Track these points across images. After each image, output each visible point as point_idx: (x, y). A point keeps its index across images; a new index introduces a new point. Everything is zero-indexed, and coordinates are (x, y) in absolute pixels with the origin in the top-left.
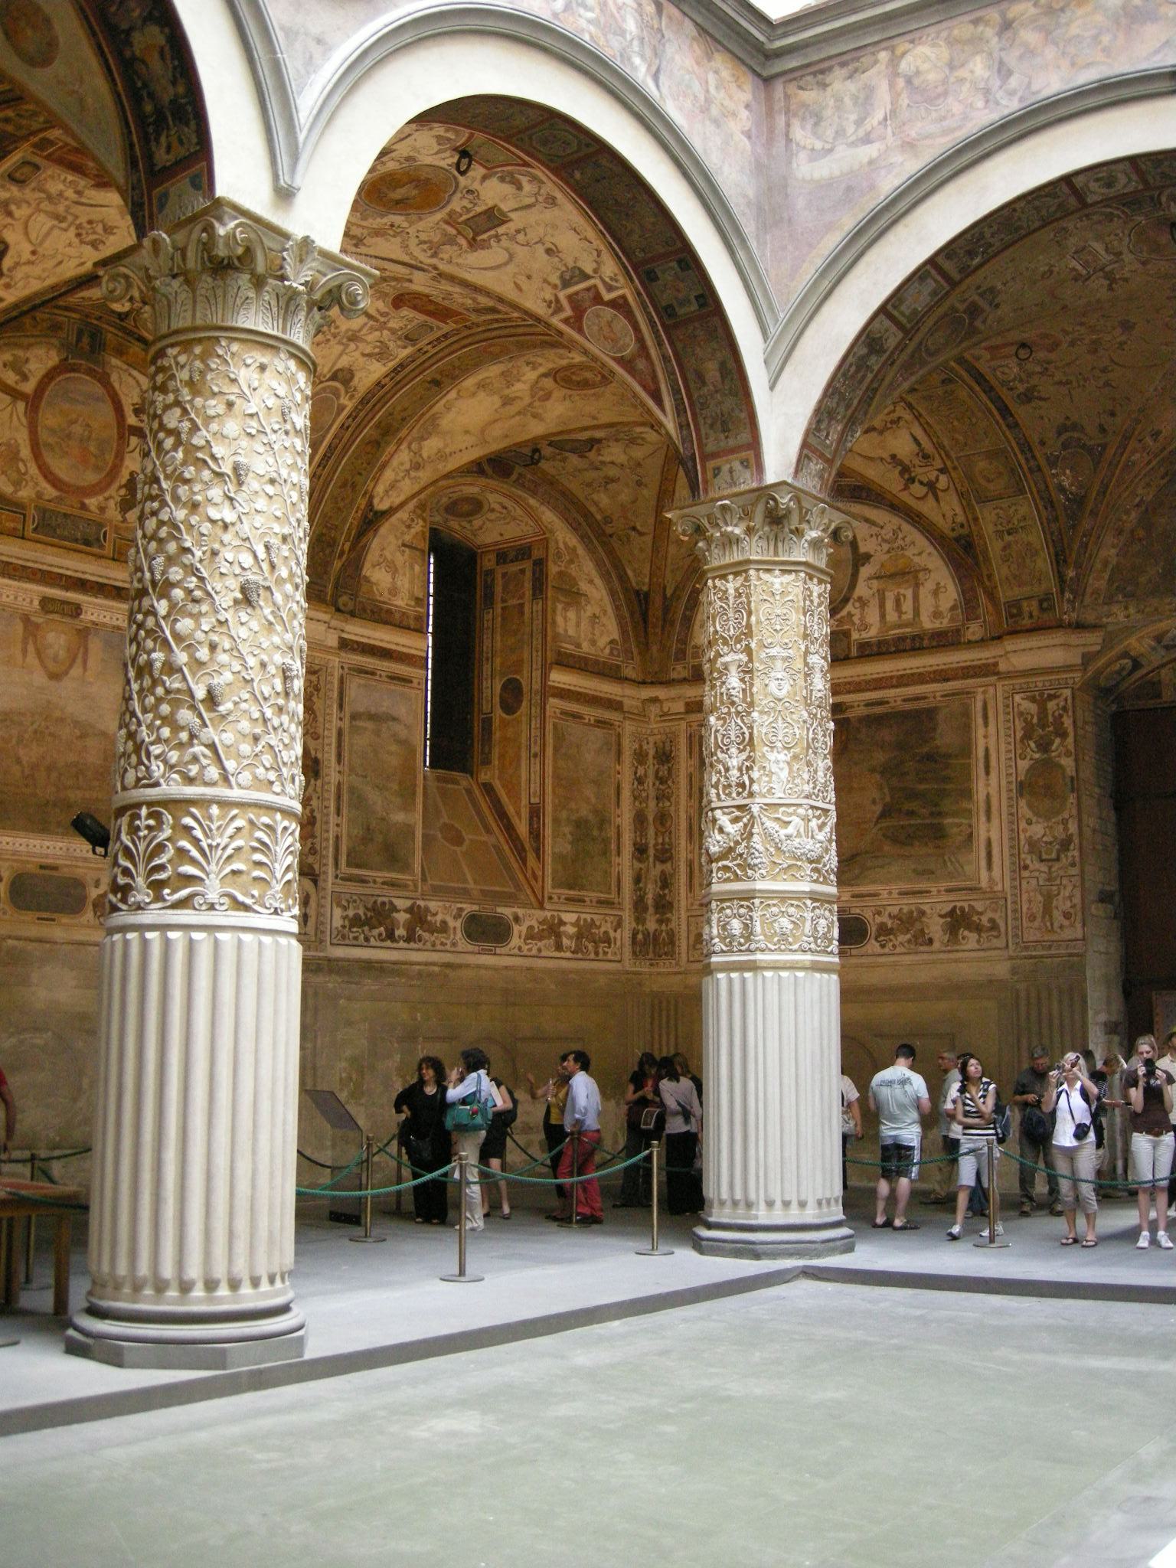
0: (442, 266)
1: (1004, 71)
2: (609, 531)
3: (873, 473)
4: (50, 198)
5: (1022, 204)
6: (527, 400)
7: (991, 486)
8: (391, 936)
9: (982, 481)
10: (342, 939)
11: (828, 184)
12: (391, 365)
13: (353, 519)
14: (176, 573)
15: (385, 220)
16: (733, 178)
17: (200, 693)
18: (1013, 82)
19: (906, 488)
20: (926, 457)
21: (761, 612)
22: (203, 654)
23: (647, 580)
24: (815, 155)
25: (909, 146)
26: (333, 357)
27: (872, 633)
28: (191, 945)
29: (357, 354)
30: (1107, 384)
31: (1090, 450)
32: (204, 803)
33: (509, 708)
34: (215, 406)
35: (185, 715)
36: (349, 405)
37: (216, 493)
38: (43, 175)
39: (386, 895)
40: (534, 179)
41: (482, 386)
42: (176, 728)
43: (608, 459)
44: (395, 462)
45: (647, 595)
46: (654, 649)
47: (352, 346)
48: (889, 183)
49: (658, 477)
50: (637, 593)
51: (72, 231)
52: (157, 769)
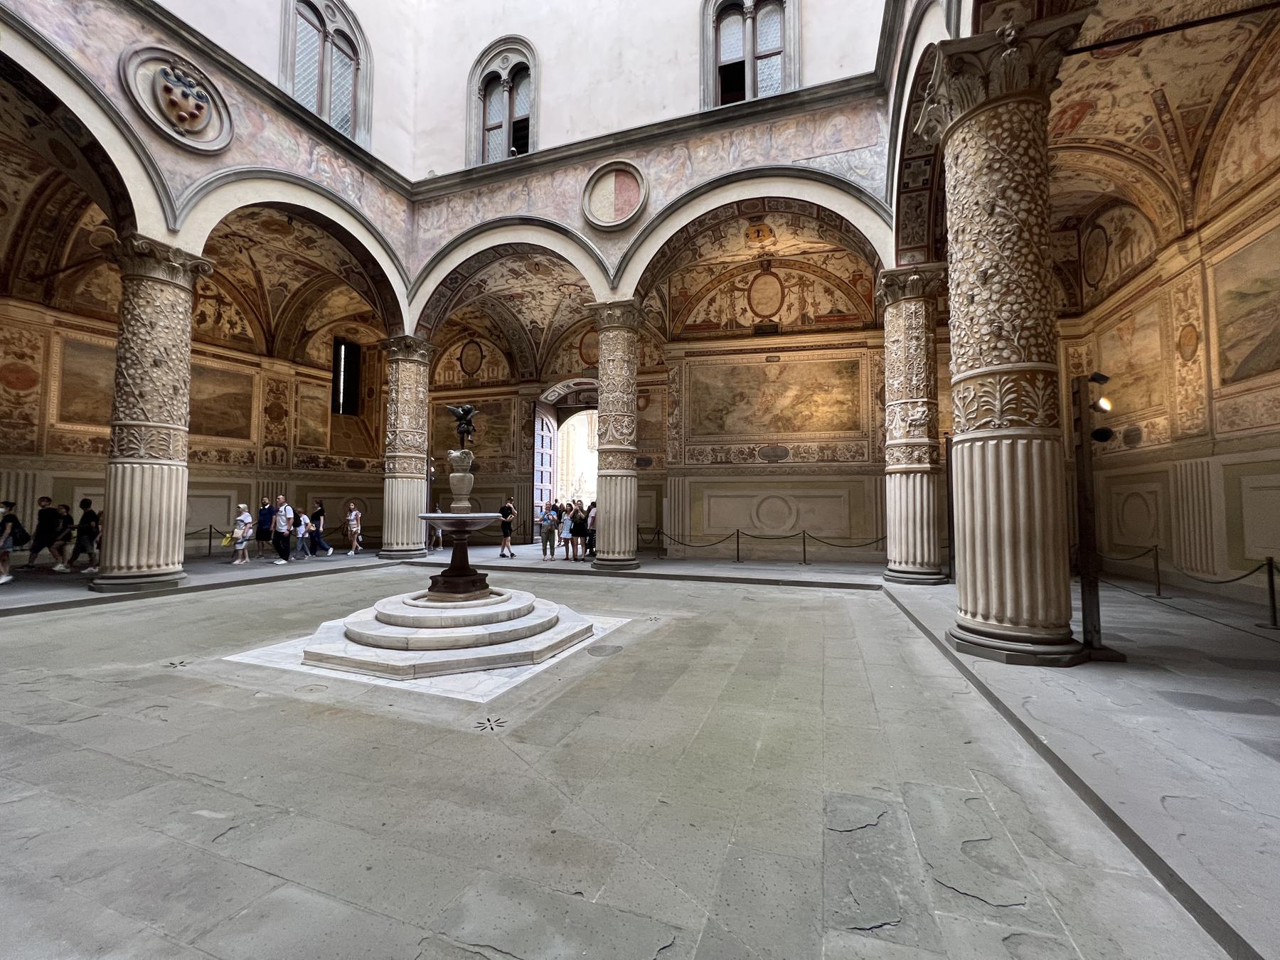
1: (478, 211)
3: (480, 330)
8: (317, 466)
10: (297, 466)
11: (427, 241)
13: (298, 332)
14: (128, 355)
16: (393, 237)
17: (137, 392)
18: (480, 215)
21: (402, 375)
22: (138, 381)
24: (426, 231)
25: (450, 231)
28: (133, 469)
32: (140, 426)
33: (370, 396)
34: (142, 302)
35: (132, 399)
37: (143, 330)
39: (314, 454)
41: (340, 292)
42: (128, 403)
48: (444, 243)
52: (122, 416)
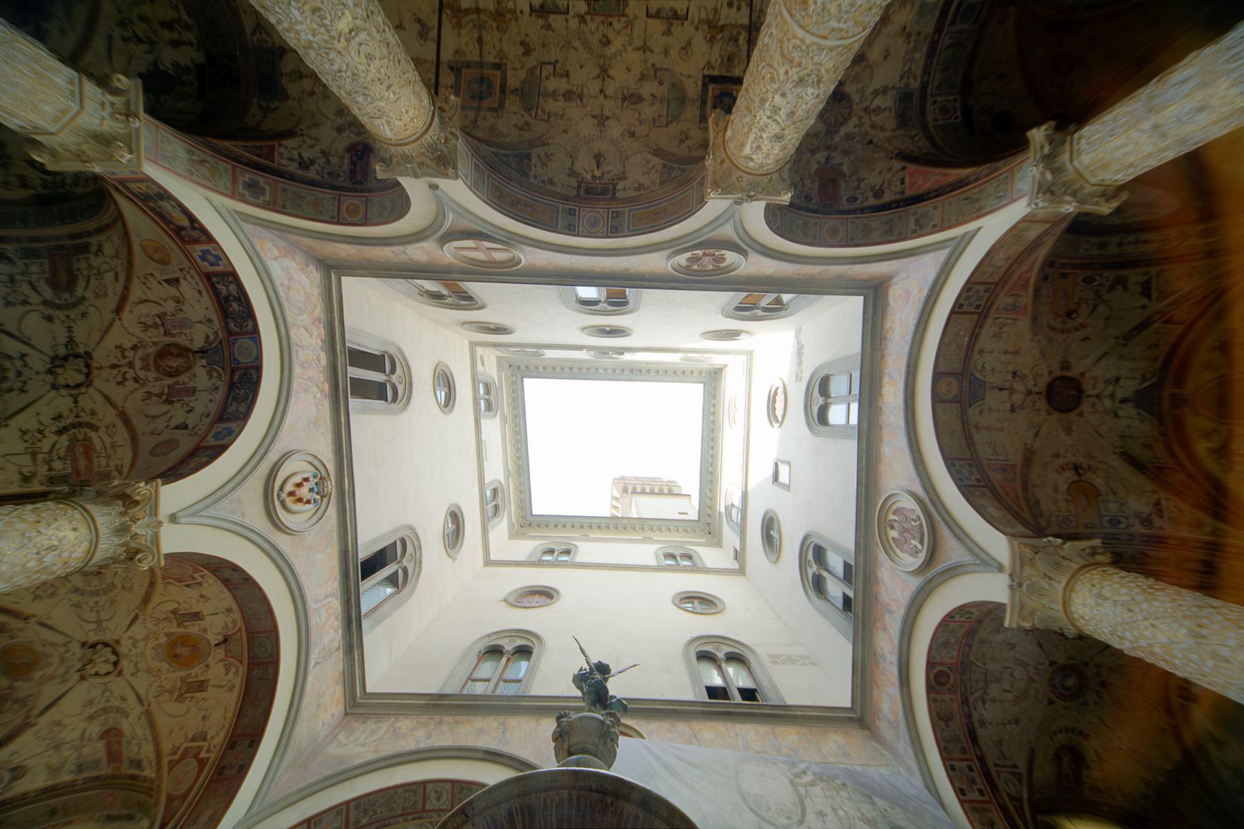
5: (400, 790)
12: (51, 783)
40: (237, 672)
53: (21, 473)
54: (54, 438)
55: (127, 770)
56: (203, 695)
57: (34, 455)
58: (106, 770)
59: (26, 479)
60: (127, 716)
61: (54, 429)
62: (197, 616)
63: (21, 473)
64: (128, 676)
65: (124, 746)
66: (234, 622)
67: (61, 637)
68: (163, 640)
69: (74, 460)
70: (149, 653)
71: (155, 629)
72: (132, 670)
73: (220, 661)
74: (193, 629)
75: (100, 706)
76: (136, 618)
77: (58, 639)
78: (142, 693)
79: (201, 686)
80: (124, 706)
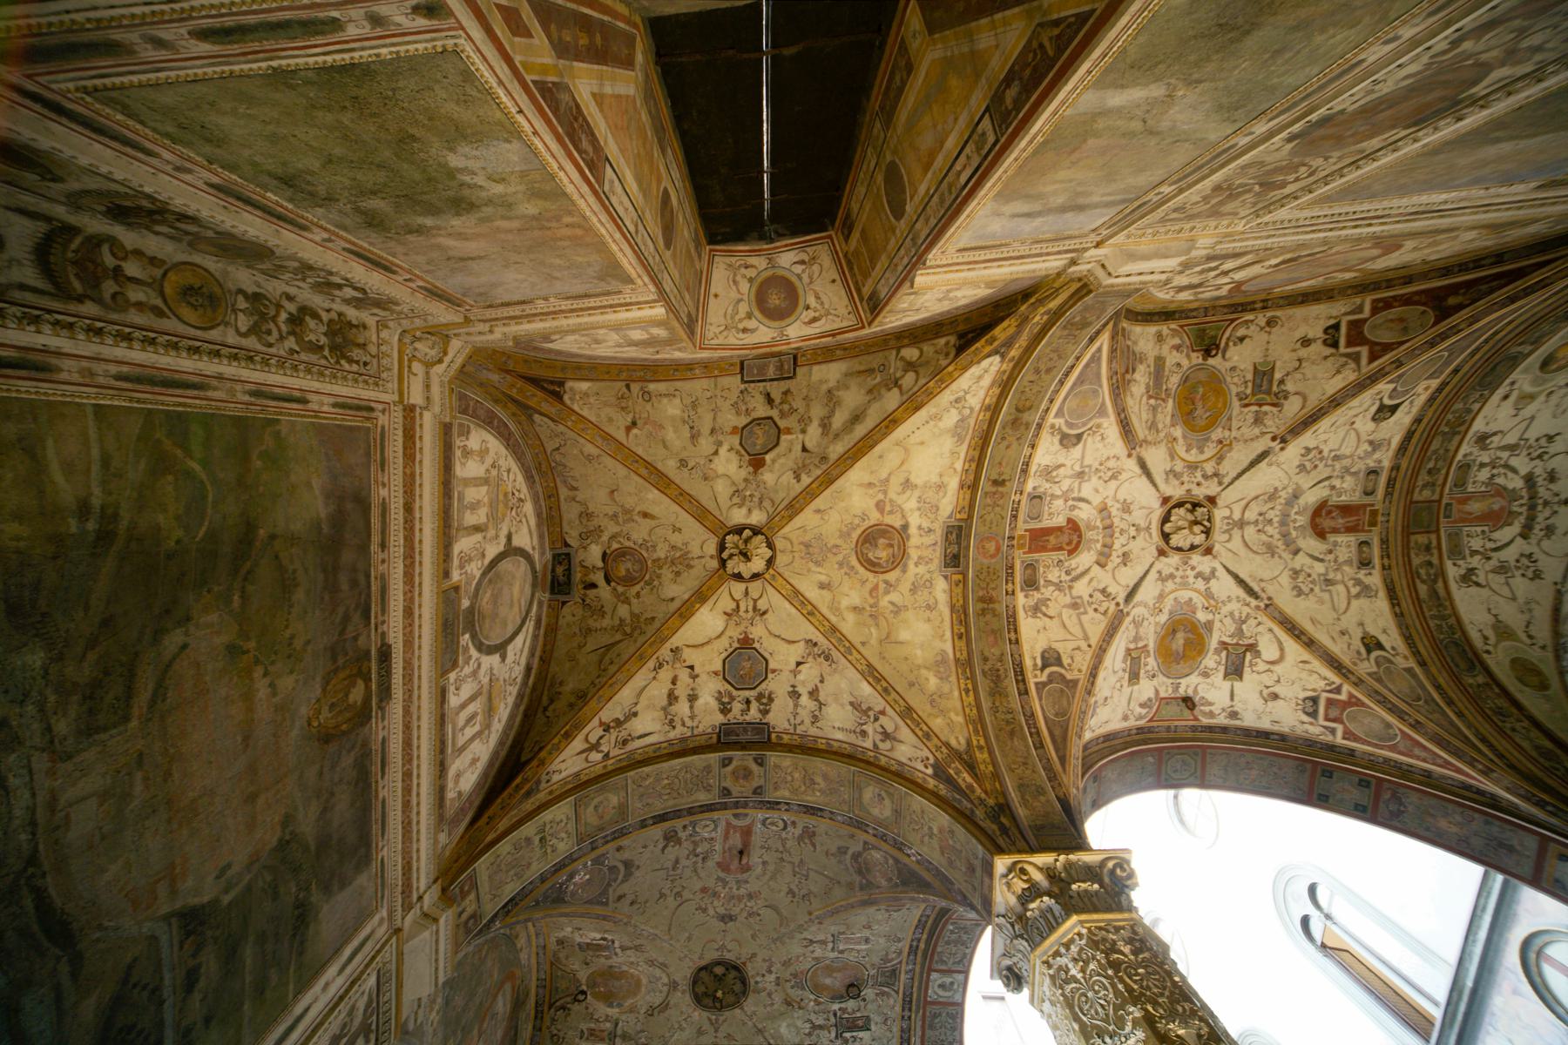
0: (1128, 620)
2: (635, 387)
4: (1347, 470)
6: (892, 495)
7: (591, 809)
9: (596, 801)
12: (1033, 468)
15: (1166, 611)
19: (601, 724)
20: (625, 742)
23: (576, 407)
26: (1088, 452)
27: (454, 701)
29: (1069, 463)
30: (662, 895)
31: (604, 892)
36: (1051, 419)
38: (1359, 488)
40: (1140, 717)
43: (723, 451)
44: (982, 393)
45: (558, 396)
46: (495, 377)
47: (1077, 468)
49: (685, 487)
50: (561, 384)
51: (1325, 454)
53: (1495, 434)
54: (1523, 471)
55: (1020, 558)
56: (1125, 683)
57: (1512, 448)
58: (1022, 526)
59: (1482, 440)
60: (1102, 566)
61: (1538, 471)
62: (1235, 671)
63: (1495, 434)
64: (1158, 566)
65: (1056, 556)
66: (1211, 715)
67: (1233, 474)
68: (1202, 616)
69: (1483, 496)
70: (1185, 595)
71: (1225, 610)
72: (1166, 572)
73: (1157, 692)
74: (1210, 661)
75: (1116, 521)
76: (1250, 591)
77: (1229, 467)
78: (1138, 597)
79: (1134, 677)
80: (1115, 559)
